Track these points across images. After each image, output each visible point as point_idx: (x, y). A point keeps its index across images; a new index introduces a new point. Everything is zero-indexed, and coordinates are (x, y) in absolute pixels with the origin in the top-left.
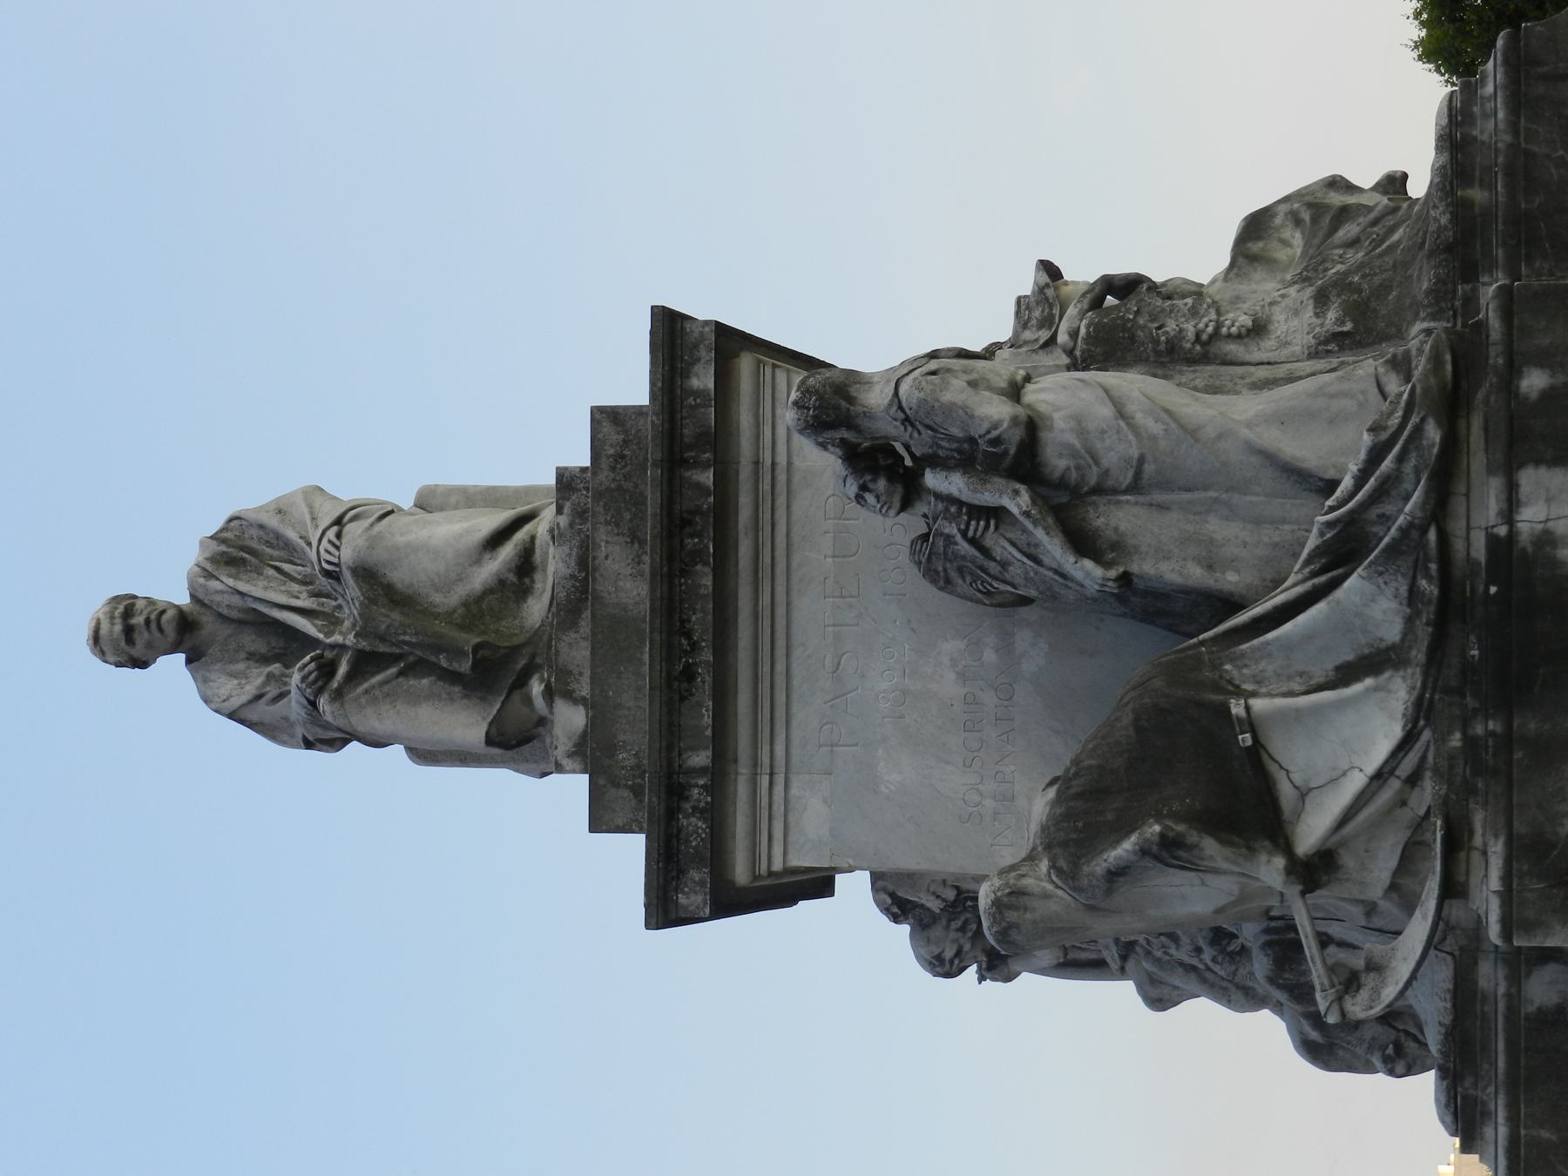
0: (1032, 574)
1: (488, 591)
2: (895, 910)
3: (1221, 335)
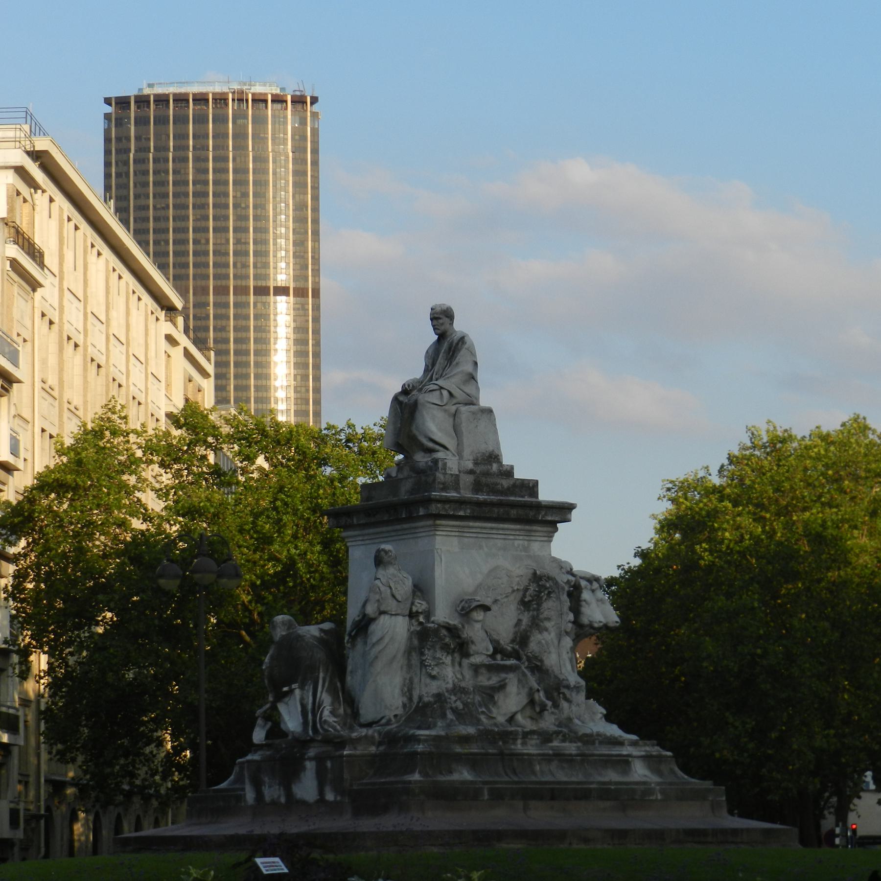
1: (418, 440)
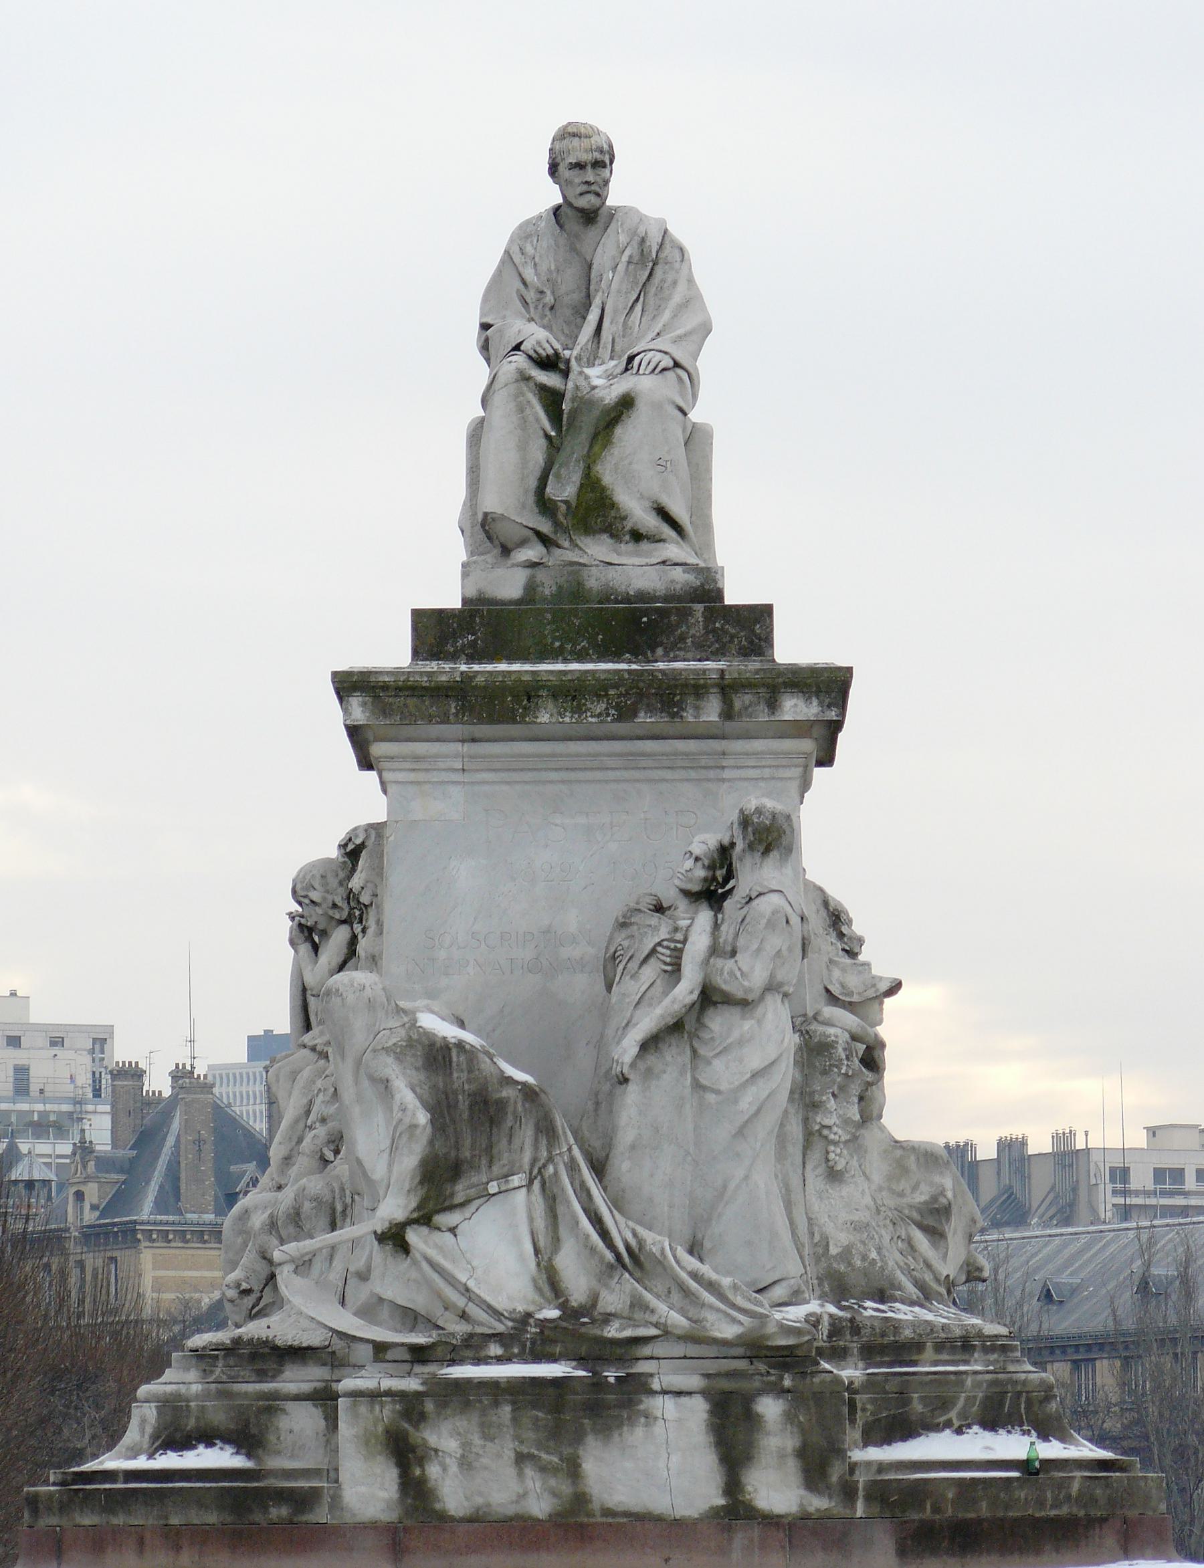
0: (627, 1000)
2: (350, 847)
3: (828, 1145)
